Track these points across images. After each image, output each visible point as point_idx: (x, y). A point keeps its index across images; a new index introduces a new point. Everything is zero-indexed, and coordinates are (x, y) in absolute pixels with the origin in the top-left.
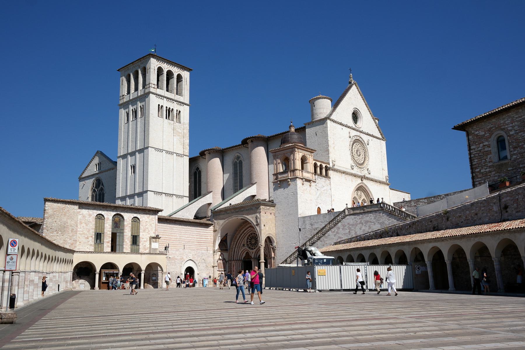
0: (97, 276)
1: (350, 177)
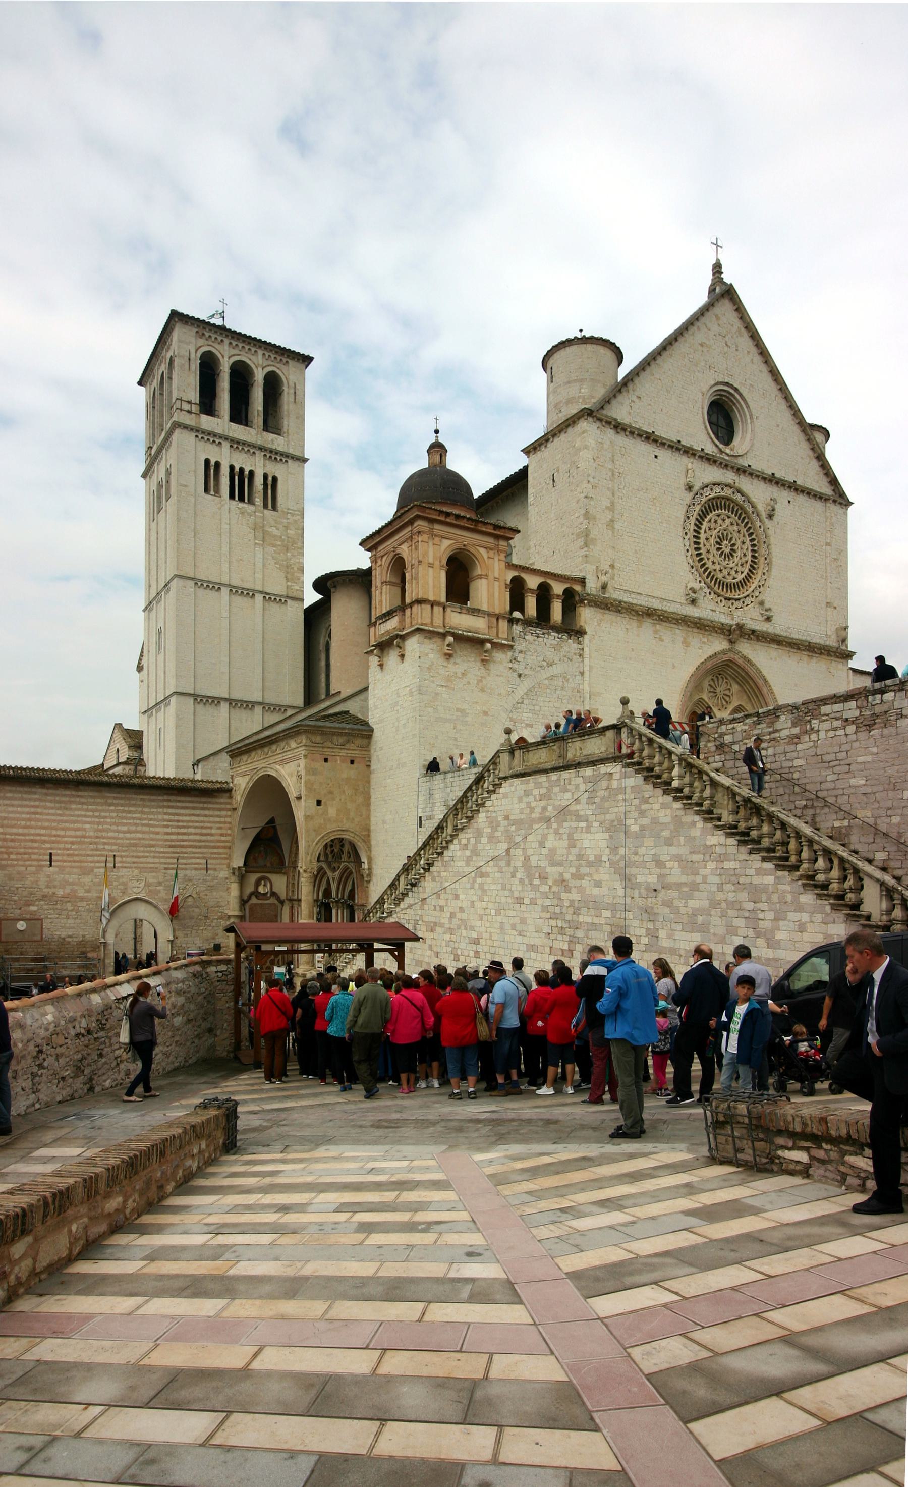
1: (679, 633)
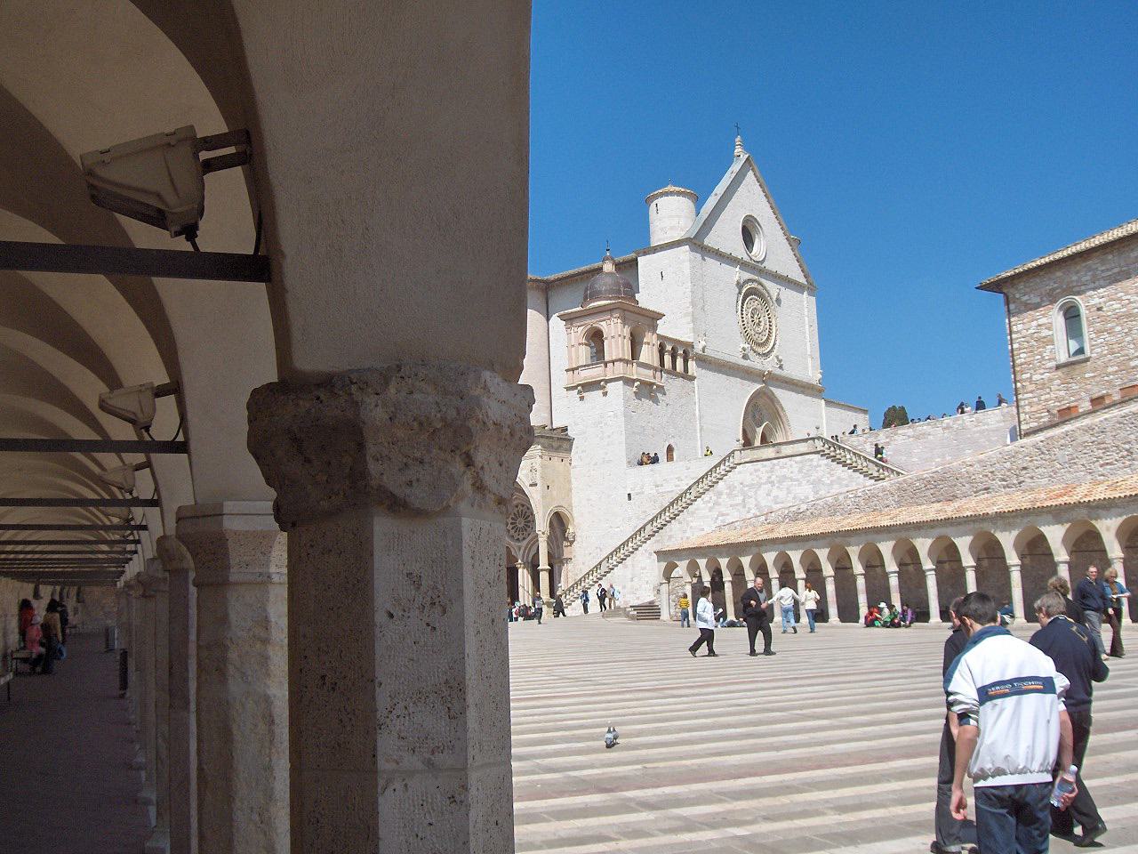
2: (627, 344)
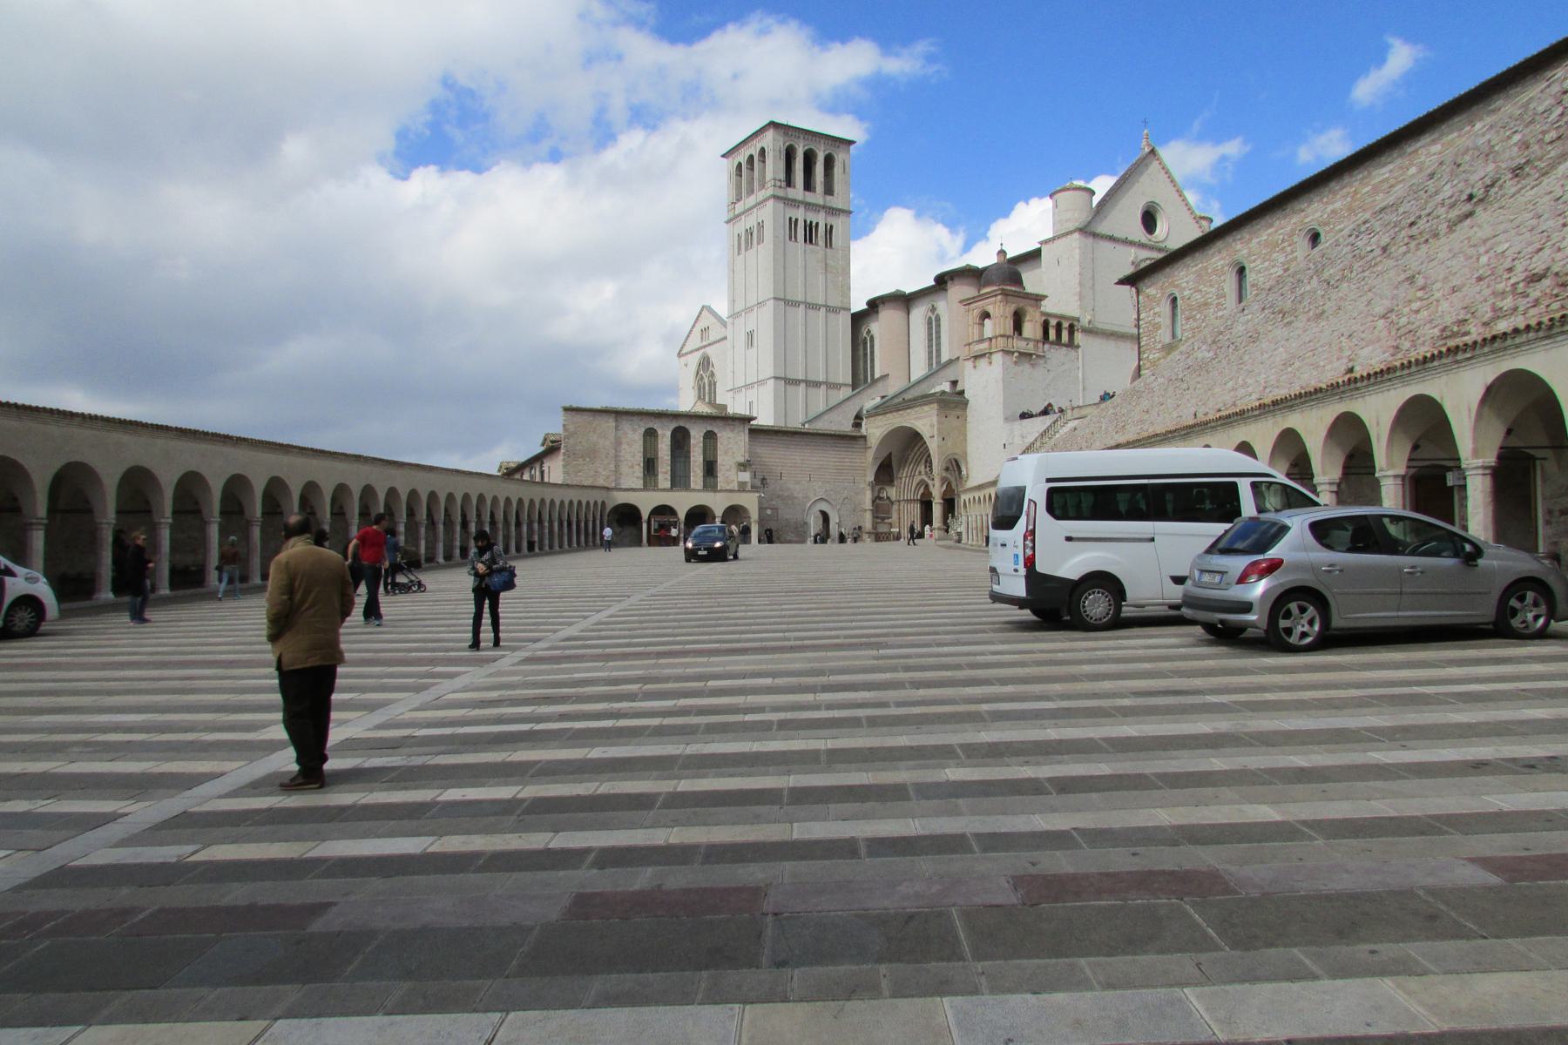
0: (645, 526)
2: (1010, 323)
